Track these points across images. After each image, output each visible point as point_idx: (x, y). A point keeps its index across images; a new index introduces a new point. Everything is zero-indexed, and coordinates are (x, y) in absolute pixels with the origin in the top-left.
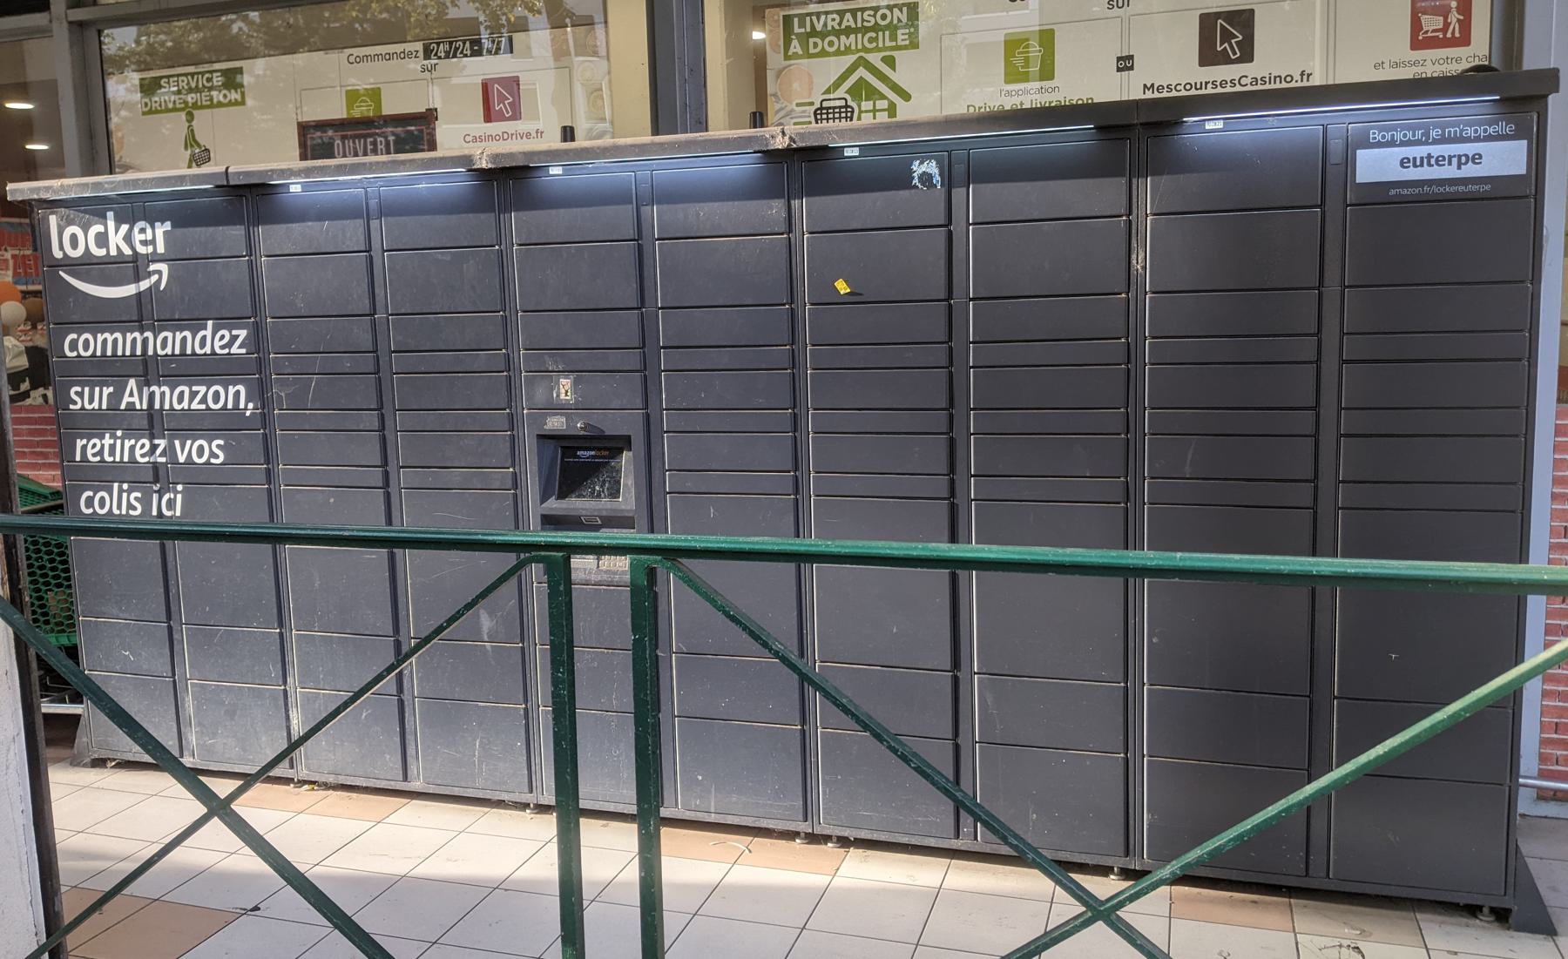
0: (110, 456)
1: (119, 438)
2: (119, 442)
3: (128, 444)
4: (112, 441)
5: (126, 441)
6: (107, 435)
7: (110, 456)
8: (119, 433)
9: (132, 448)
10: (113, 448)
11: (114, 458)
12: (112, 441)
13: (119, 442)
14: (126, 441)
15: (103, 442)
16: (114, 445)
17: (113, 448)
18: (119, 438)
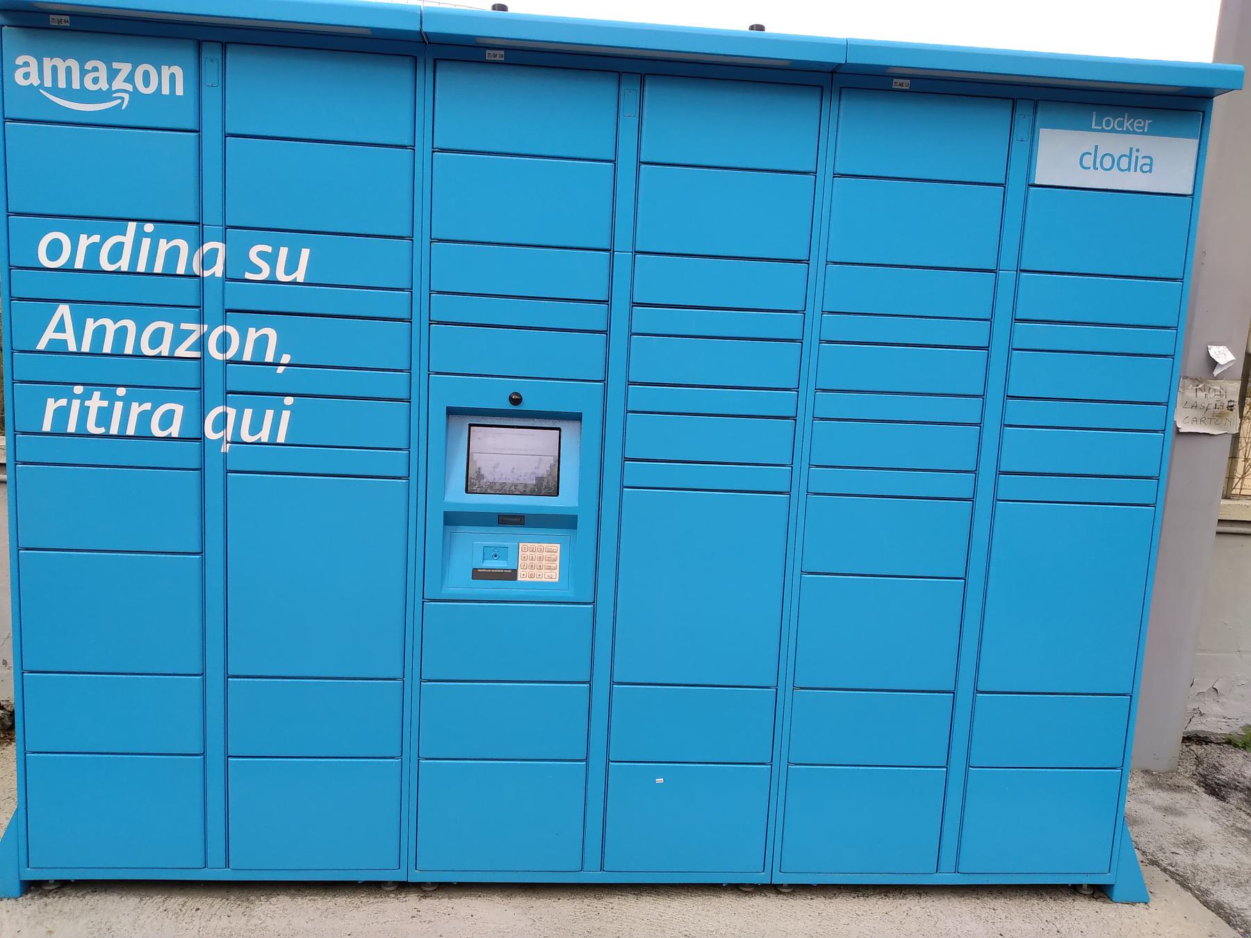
0: (98, 425)
1: (120, 399)
2: (119, 406)
3: (136, 409)
4: (105, 404)
5: (135, 405)
6: (97, 395)
7: (98, 425)
8: (121, 391)
9: (145, 418)
10: (104, 417)
11: (108, 428)
12: (105, 404)
13: (119, 406)
14: (135, 405)
15: (87, 403)
16: (110, 410)
17: (104, 417)
18: (120, 399)
